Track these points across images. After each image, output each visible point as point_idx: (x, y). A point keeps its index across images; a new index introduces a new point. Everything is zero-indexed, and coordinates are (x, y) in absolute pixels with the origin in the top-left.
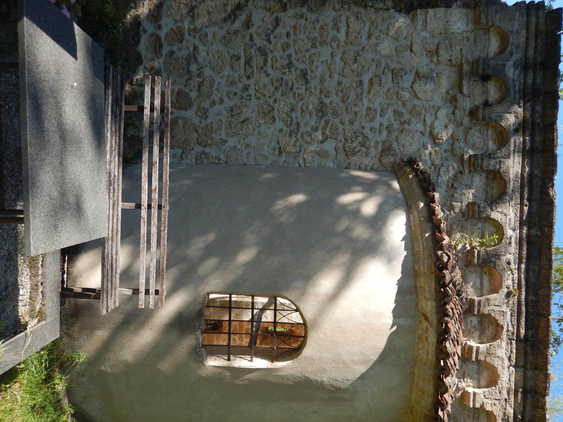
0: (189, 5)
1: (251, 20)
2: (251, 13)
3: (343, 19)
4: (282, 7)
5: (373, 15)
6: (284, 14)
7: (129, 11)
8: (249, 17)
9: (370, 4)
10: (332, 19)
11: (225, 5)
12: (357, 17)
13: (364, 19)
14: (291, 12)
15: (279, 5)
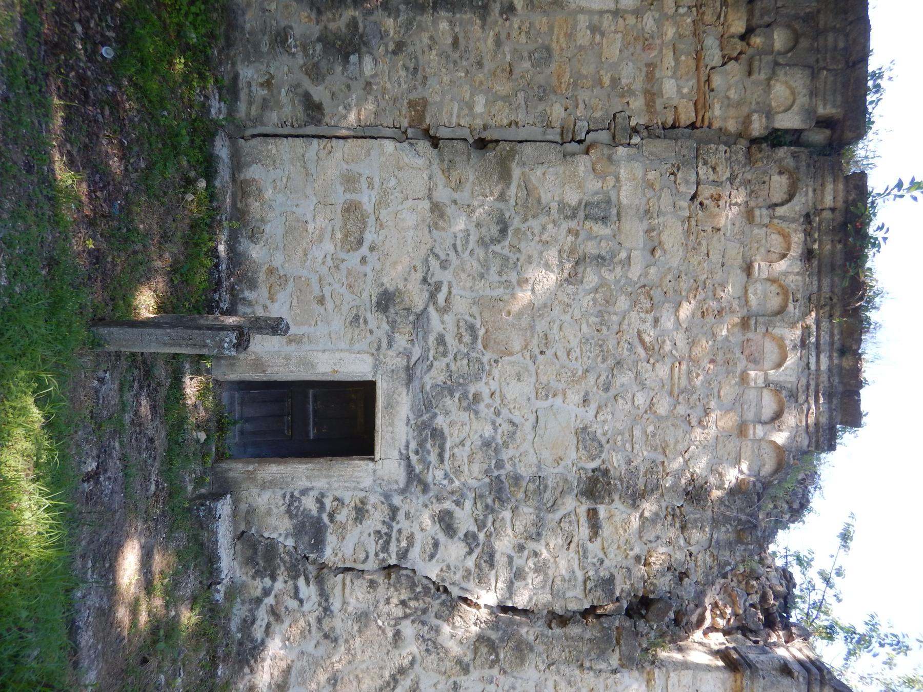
0: (329, 669)
1: (418, 687)
2: (418, 677)
3: (550, 684)
4: (464, 669)
5: (593, 679)
6: (466, 678)
7: (243, 678)
8: (417, 683)
9: (587, 664)
10: (534, 684)
11: (381, 668)
12: (569, 683)
13: (580, 684)
14: (475, 674)
15: (458, 667)
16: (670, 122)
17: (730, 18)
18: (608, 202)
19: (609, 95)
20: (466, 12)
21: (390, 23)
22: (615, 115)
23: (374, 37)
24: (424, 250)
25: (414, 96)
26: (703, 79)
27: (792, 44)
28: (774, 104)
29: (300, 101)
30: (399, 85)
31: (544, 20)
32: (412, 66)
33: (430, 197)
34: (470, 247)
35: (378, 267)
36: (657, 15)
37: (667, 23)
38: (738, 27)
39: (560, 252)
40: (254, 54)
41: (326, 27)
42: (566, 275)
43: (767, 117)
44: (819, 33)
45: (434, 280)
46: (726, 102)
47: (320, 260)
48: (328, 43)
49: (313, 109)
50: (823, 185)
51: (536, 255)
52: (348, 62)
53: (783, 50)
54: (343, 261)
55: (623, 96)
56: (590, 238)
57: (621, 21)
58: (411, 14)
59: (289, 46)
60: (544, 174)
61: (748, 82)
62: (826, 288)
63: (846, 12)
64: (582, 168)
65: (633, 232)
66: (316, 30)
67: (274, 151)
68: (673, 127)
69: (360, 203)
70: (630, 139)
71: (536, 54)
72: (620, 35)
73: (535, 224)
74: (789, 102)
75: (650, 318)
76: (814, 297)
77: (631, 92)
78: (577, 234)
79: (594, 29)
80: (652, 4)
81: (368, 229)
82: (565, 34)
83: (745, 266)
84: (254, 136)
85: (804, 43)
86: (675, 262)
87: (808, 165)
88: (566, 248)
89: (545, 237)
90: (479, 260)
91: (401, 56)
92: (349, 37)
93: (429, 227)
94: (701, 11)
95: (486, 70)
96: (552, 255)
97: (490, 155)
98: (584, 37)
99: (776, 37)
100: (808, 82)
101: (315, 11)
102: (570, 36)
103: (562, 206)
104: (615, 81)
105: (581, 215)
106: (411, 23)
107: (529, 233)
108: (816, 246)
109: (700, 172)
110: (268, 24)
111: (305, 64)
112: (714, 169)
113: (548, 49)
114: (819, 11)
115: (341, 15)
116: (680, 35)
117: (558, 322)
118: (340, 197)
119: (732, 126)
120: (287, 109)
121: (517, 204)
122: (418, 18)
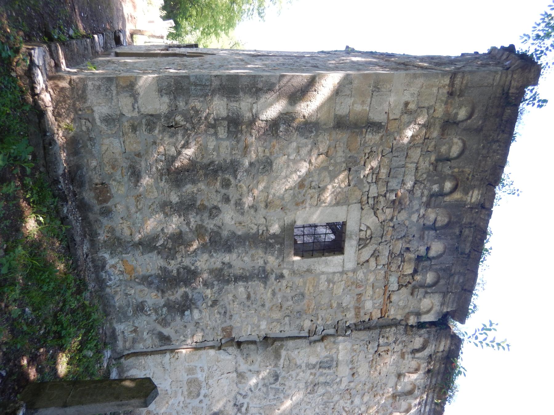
16: (367, 320)
17: (405, 267)
18: (332, 360)
19: (335, 312)
20: (254, 281)
21: (208, 292)
22: (338, 322)
23: (199, 300)
24: (234, 393)
25: (224, 325)
26: (387, 295)
27: (435, 280)
28: (422, 307)
29: (156, 337)
30: (216, 321)
31: (301, 280)
32: (223, 312)
33: (236, 371)
34: (259, 388)
35: (209, 403)
36: (365, 271)
37: (370, 275)
38: (410, 271)
39: (306, 383)
40: (123, 317)
41: (168, 299)
42: (309, 391)
43: (418, 318)
44: (452, 275)
45: (240, 403)
46: (397, 307)
47: (176, 405)
48: (171, 307)
49: (165, 339)
50: (440, 342)
51: (293, 385)
52: (184, 315)
53: (431, 283)
54: (189, 403)
55: (343, 312)
56: (322, 375)
57: (345, 276)
58: (221, 286)
59: (146, 311)
60: (299, 352)
61: (411, 297)
62: (434, 382)
63: (466, 265)
64: (319, 349)
65: (344, 371)
66: (162, 302)
67: (143, 363)
68: (369, 320)
69: (197, 378)
70: (346, 332)
71: (296, 298)
72: (344, 282)
73: (294, 373)
74: (430, 307)
75: (349, 402)
76: (427, 387)
77: (347, 309)
78: (315, 375)
79: (329, 281)
80: (363, 264)
81: (202, 389)
82: (313, 286)
83: (397, 375)
84: (128, 355)
85: (442, 282)
86: (363, 379)
87: (434, 336)
88: (309, 381)
89: (298, 378)
90: (263, 392)
91: (216, 307)
92: (183, 303)
93: (237, 383)
94: (390, 266)
95: (266, 308)
96: (302, 385)
97: (270, 349)
98: (323, 286)
99: (428, 276)
100: (441, 299)
101: (160, 292)
102: (315, 286)
103: (308, 365)
104: (340, 305)
105: (318, 366)
106: (221, 290)
107: (290, 378)
108: (432, 367)
109: (380, 341)
110: (131, 302)
111: (157, 319)
112: (387, 338)
113: (303, 295)
114: (453, 264)
115: (177, 292)
116: (377, 280)
117: (304, 409)
118: (185, 377)
119: (399, 317)
120: (148, 342)
121: (283, 367)
122: (226, 287)
